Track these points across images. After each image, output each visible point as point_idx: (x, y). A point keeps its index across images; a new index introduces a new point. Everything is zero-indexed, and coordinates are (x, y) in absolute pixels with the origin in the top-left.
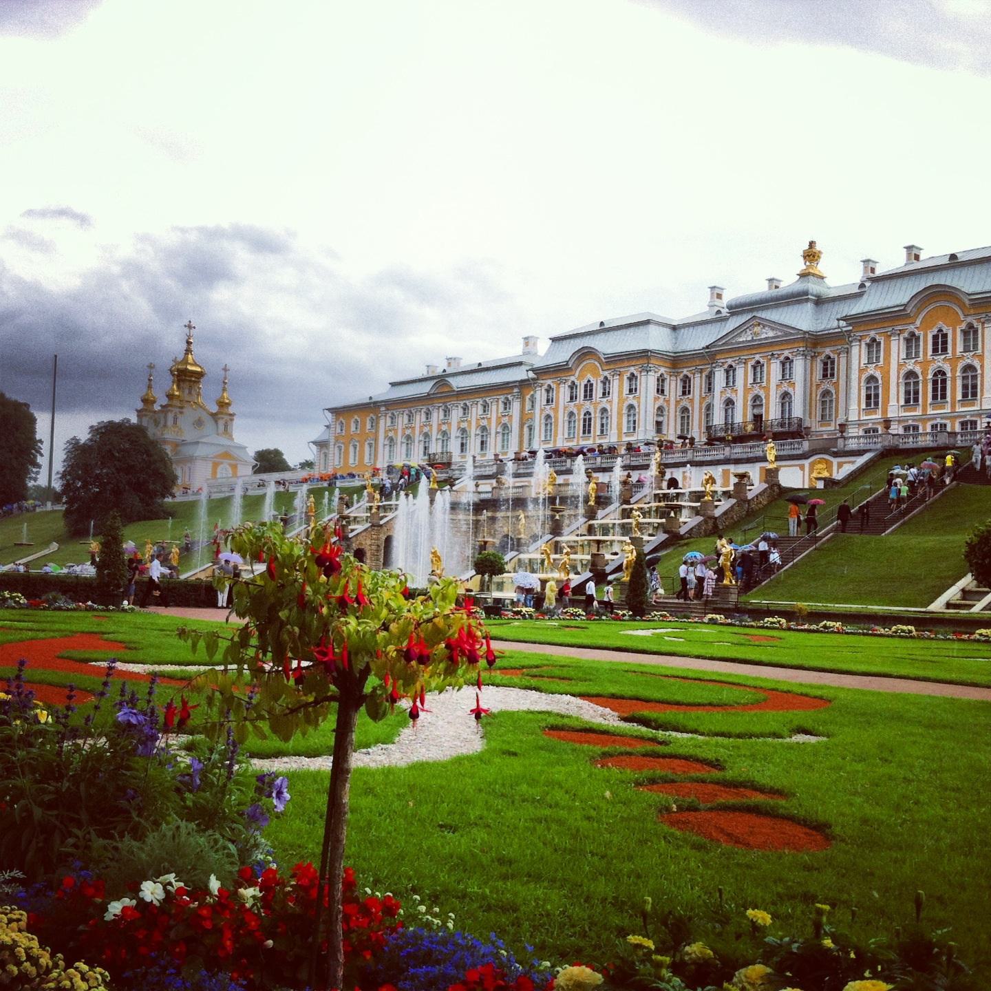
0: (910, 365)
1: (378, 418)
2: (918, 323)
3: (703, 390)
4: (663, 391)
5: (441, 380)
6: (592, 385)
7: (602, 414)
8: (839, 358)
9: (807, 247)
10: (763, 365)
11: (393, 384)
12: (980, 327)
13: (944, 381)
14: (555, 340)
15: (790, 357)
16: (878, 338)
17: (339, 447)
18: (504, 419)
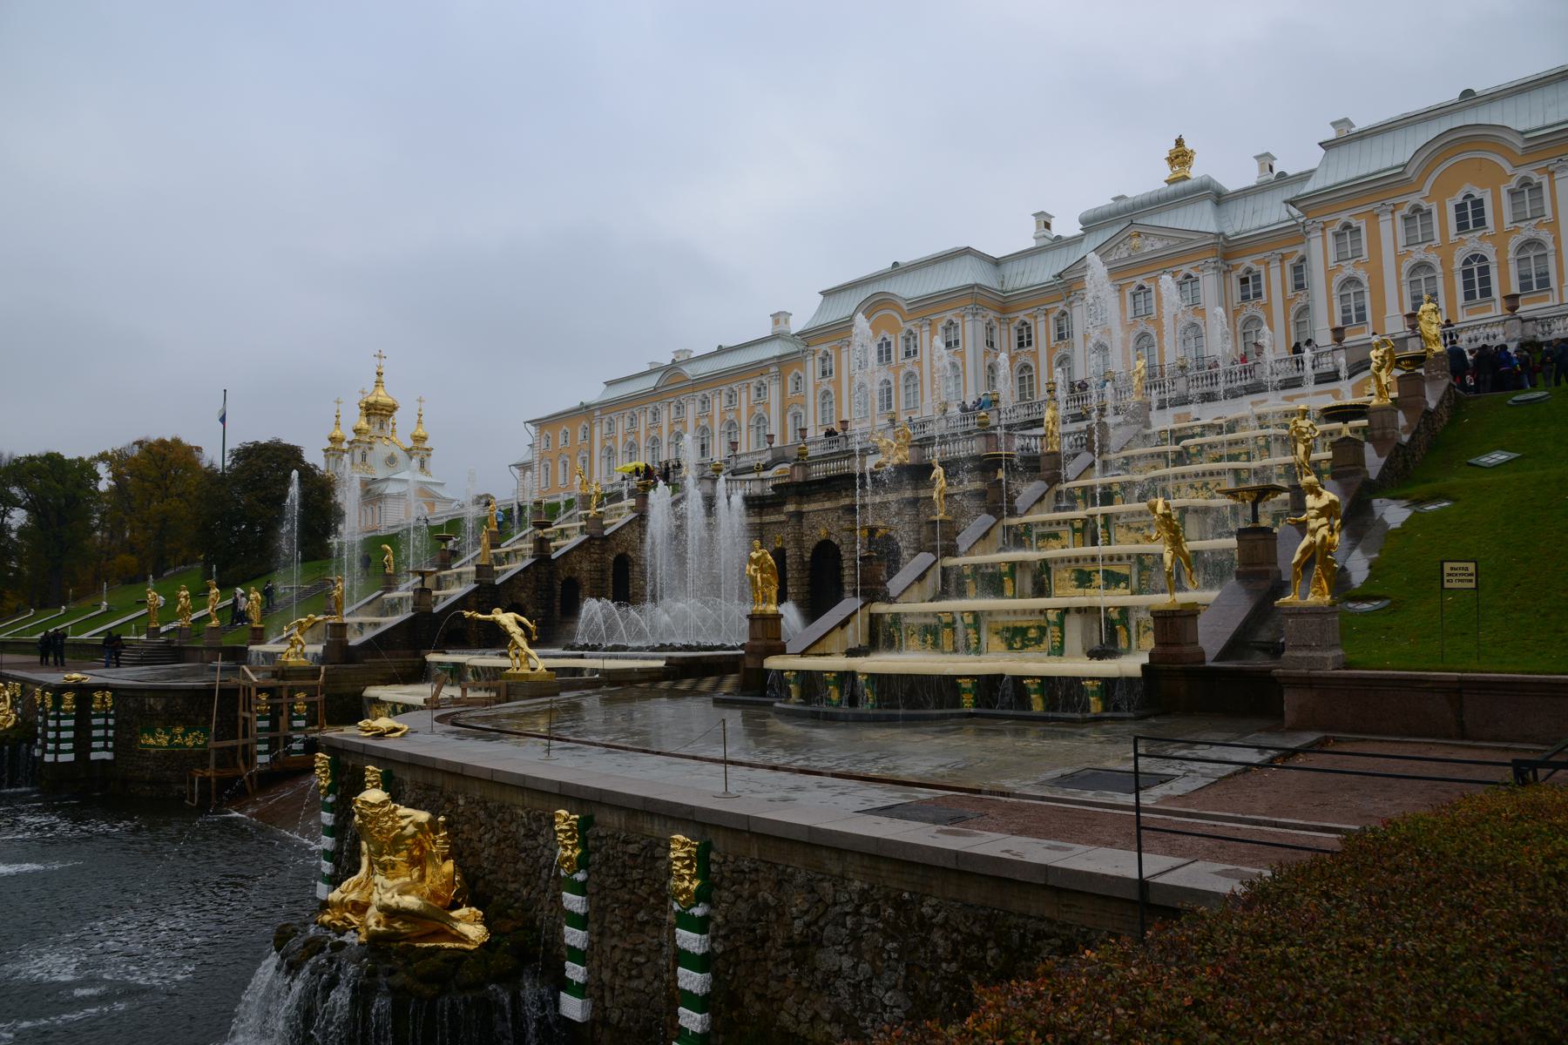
0: (1418, 254)
1: (592, 425)
2: (1426, 190)
3: (1052, 338)
4: (992, 344)
5: (671, 371)
6: (889, 344)
7: (907, 380)
8: (1267, 271)
9: (1173, 146)
10: (1150, 291)
11: (609, 384)
12: (1545, 181)
13: (1484, 271)
14: (826, 294)
15: (1194, 274)
16: (1354, 223)
17: (545, 465)
18: (759, 408)
